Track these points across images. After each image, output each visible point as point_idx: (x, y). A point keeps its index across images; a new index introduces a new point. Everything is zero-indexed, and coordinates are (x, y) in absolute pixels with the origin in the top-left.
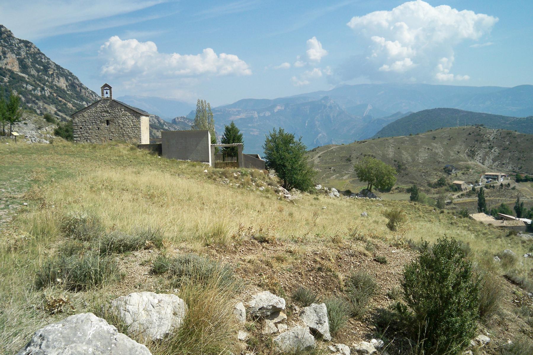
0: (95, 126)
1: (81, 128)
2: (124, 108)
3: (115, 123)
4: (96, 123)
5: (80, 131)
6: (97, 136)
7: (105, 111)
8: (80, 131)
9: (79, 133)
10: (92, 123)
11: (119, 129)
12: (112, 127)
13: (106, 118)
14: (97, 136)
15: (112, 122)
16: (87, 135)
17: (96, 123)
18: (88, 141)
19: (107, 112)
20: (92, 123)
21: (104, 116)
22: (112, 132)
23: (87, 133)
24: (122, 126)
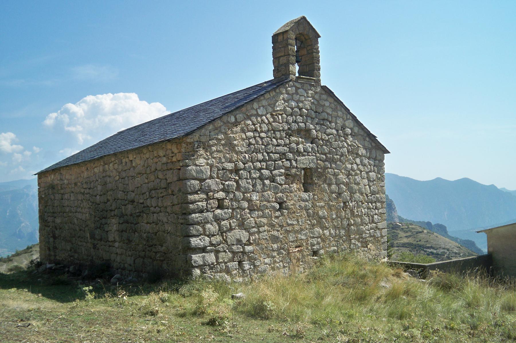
0: (269, 194)
1: (220, 206)
2: (349, 123)
3: (330, 185)
4: (273, 179)
5: (218, 220)
6: (275, 239)
7: (299, 132)
8: (218, 220)
9: (212, 228)
10: (262, 178)
11: (338, 210)
12: (321, 201)
13: (305, 161)
14: (275, 239)
15: (320, 176)
16: (244, 235)
17: (273, 179)
18: (247, 266)
19: (305, 134)
20: (262, 178)
21: (298, 153)
22: (320, 221)
23: (242, 225)
24: (346, 195)
